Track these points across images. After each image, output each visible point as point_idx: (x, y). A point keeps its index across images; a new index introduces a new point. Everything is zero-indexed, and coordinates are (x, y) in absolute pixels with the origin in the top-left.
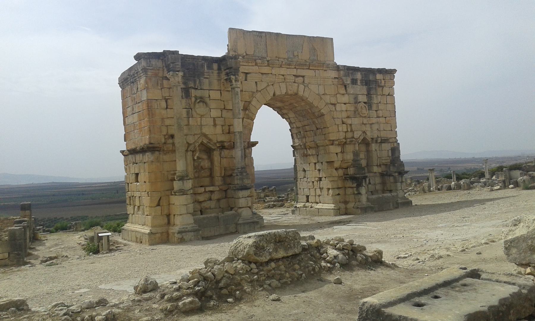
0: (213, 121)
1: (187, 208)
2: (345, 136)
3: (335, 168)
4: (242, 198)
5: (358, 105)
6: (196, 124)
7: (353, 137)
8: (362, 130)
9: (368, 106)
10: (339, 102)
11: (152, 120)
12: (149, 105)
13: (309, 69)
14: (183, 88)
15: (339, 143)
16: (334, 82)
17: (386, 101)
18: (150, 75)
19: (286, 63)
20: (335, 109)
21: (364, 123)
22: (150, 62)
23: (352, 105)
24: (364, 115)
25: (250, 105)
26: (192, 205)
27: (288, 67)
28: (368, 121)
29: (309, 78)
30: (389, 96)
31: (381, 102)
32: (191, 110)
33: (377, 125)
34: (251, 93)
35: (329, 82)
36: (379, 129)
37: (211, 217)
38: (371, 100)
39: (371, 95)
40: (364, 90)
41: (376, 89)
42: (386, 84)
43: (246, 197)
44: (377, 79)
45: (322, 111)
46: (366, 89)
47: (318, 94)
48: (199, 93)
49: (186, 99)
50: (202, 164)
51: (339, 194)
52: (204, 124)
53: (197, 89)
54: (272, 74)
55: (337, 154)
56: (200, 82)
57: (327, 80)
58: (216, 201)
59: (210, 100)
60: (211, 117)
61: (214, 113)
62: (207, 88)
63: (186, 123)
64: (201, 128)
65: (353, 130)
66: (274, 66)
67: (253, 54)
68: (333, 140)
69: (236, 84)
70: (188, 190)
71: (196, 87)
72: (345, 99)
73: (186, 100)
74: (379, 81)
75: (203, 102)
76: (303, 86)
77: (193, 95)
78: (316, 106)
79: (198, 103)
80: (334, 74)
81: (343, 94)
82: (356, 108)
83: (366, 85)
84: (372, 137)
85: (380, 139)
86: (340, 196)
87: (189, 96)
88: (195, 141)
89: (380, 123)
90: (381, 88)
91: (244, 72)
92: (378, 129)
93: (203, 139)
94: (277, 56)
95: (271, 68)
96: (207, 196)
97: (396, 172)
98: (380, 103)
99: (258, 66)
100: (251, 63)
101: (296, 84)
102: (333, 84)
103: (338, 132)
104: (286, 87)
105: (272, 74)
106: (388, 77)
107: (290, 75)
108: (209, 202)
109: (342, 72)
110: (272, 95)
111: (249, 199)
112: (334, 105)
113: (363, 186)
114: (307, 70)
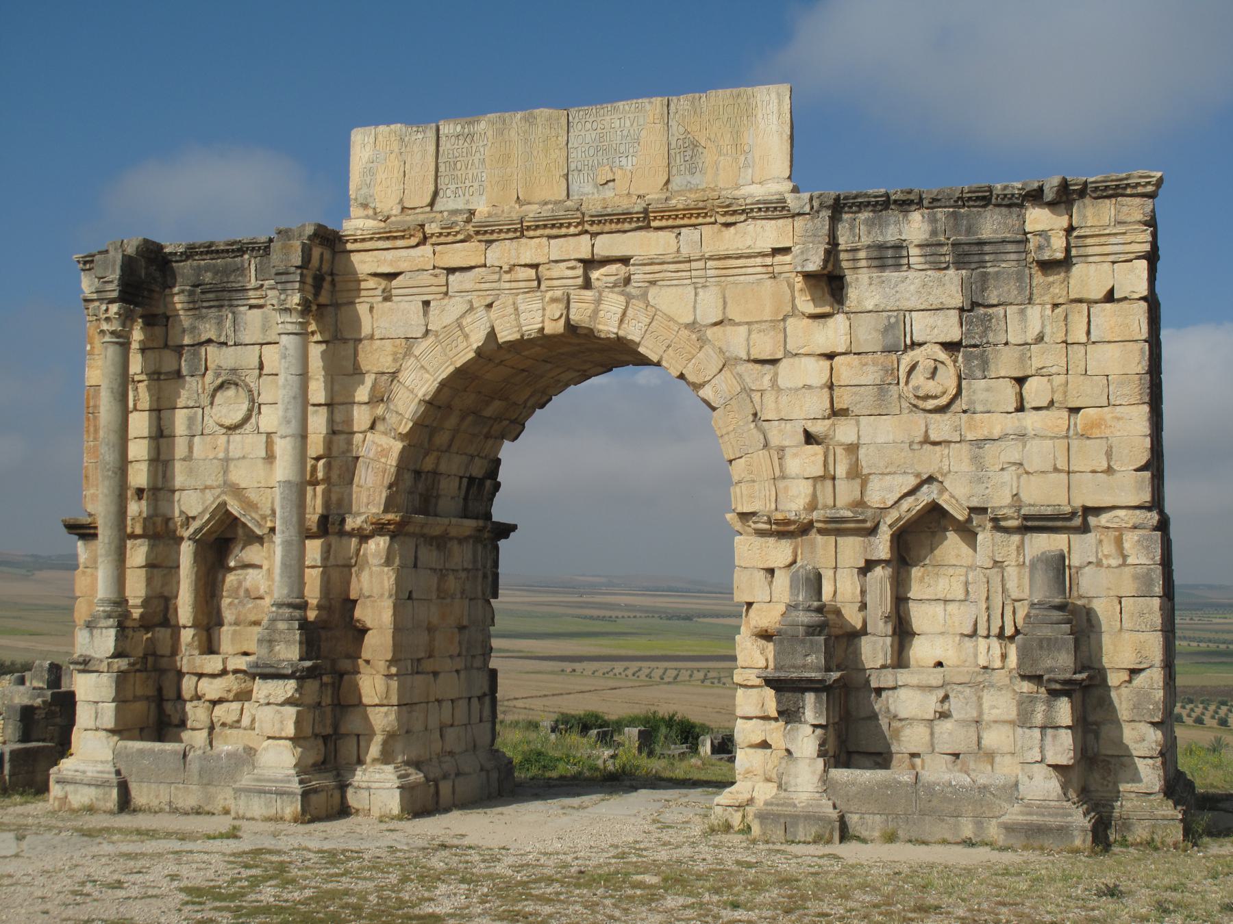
0: (263, 446)
1: (97, 713)
2: (814, 496)
4: (268, 704)
6: (211, 457)
7: (860, 504)
8: (920, 469)
9: (968, 359)
11: (94, 446)
12: (91, 404)
13: (648, 227)
16: (777, 269)
17: (1088, 333)
20: (774, 381)
21: (934, 437)
24: (931, 404)
26: (114, 704)
27: (555, 232)
28: (957, 428)
30: (1108, 305)
32: (200, 411)
35: (750, 270)
37: (163, 751)
38: (987, 329)
42: (1090, 251)
46: (957, 281)
47: (692, 326)
51: (765, 745)
53: (225, 344)
55: (771, 571)
59: (260, 375)
60: (261, 430)
65: (865, 471)
66: (495, 236)
70: (101, 661)
71: (222, 339)
72: (834, 334)
76: (622, 299)
82: (893, 371)
83: (959, 264)
84: (975, 503)
86: (769, 751)
91: (380, 270)
93: (224, 504)
98: (1040, 339)
101: (588, 294)
103: (784, 477)
108: (236, 706)
110: (477, 339)
112: (774, 362)
113: (806, 722)
114: (643, 233)
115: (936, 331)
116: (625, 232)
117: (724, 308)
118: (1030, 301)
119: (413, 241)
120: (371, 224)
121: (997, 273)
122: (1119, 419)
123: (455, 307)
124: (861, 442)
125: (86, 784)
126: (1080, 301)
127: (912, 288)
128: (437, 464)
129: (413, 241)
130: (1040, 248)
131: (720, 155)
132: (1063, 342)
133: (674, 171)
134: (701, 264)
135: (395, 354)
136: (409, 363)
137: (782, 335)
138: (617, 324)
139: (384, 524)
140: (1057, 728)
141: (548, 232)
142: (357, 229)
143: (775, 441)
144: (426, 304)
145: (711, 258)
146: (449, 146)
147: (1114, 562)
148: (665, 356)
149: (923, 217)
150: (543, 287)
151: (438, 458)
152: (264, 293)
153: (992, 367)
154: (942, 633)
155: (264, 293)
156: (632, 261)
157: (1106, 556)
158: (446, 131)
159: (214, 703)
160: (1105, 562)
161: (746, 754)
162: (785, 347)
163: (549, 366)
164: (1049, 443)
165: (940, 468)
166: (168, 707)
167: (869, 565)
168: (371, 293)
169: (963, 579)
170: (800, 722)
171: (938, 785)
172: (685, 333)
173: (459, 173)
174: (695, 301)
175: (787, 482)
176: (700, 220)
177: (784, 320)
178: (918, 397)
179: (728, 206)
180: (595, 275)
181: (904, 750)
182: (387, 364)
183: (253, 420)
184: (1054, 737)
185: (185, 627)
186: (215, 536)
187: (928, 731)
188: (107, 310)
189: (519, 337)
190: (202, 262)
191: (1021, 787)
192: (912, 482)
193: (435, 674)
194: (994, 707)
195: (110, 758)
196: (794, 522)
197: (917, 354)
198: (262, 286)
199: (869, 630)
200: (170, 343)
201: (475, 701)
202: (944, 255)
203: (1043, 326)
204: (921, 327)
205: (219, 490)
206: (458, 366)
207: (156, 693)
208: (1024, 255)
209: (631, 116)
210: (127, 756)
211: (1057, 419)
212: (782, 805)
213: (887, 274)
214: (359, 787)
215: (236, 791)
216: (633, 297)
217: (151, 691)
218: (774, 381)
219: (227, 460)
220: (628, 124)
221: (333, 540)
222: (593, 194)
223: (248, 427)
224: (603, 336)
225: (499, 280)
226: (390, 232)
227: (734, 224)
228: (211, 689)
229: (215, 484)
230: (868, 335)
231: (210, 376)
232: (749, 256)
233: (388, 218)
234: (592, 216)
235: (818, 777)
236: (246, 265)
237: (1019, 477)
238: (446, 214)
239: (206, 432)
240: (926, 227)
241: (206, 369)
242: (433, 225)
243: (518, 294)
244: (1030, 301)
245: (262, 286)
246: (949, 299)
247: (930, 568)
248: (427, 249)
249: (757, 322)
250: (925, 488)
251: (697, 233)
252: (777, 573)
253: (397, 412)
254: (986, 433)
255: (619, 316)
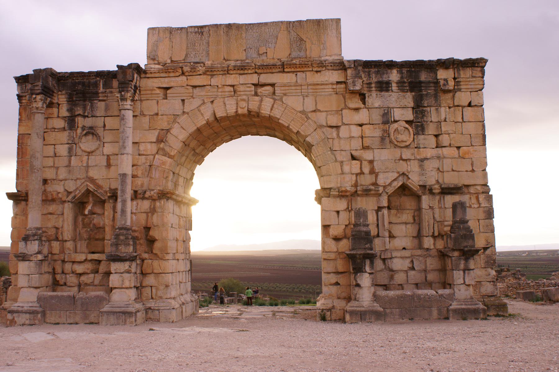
0: (105, 161)
2: (356, 181)
3: (331, 236)
4: (116, 273)
5: (392, 126)
7: (375, 184)
8: (399, 170)
9: (417, 127)
10: (345, 121)
11: (22, 161)
12: (20, 142)
13: (283, 72)
14: (68, 117)
15: (340, 193)
17: (463, 118)
18: (26, 104)
19: (235, 66)
20: (338, 135)
21: (404, 157)
22: (26, 87)
23: (377, 126)
24: (403, 144)
25: (169, 135)
26: (38, 275)
27: (242, 72)
28: (413, 154)
29: (283, 86)
30: (469, 108)
31: (447, 120)
32: (75, 146)
33: (438, 161)
34: (173, 116)
36: (441, 169)
37: (62, 296)
38: (423, 116)
39: (425, 107)
40: (409, 99)
41: (436, 96)
42: (462, 87)
43: (122, 273)
44: (438, 78)
45: (308, 139)
46: (411, 97)
47: (303, 112)
48: (89, 122)
49: (69, 131)
50: (95, 221)
51: (337, 284)
52: (93, 165)
53: (87, 116)
54: (210, 85)
56: (92, 107)
57: (322, 87)
58: (102, 275)
59: (104, 130)
60: (105, 154)
61: (108, 149)
62: (102, 113)
63: (66, 162)
64: (88, 169)
65: (377, 171)
66: (215, 73)
67: (184, 60)
68: (330, 189)
69: (122, 105)
70: (31, 255)
71: (86, 114)
72: (363, 116)
73: (69, 133)
74: (442, 82)
75: (93, 134)
76: (271, 100)
77: (80, 125)
78: (296, 131)
79: (86, 135)
80: (335, 76)
81: (357, 109)
83: (411, 91)
84: (421, 183)
85: (437, 186)
86: (339, 286)
87: (74, 126)
88: (77, 189)
89: (444, 157)
90: (451, 94)
92: (438, 169)
93: (87, 185)
94: (226, 58)
95: (210, 77)
96: (88, 267)
97: (453, 250)
98: (445, 121)
99: (186, 76)
100: (173, 72)
101: (257, 98)
102: (337, 93)
103: (343, 173)
104: (237, 104)
105: (210, 85)
106: (465, 74)
107: (246, 84)
108: (92, 276)
109: (349, 72)
110: (208, 115)
111: (126, 275)
112: (337, 127)
113: (366, 272)
114: (281, 74)
115: (403, 116)
116: (273, 73)
117: (316, 105)
118: (440, 106)
119: (177, 74)
120: (157, 66)
121: (427, 94)
122: (475, 151)
123: (196, 102)
124: (375, 159)
125: (24, 313)
126: (458, 106)
127: (393, 99)
128: (180, 171)
129: (177, 74)
130: (444, 85)
131: (312, 44)
132: (453, 121)
133: (293, 50)
134: (306, 87)
135: (168, 121)
136: (175, 125)
137: (340, 117)
138: (269, 110)
139: (165, 194)
140: (469, 270)
141: (239, 72)
142: (152, 68)
143: (339, 158)
144: (183, 101)
145: (310, 85)
146: (192, 36)
147: (476, 206)
148: (291, 124)
149: (398, 72)
150: (236, 95)
151: (180, 168)
152: (106, 95)
153: (426, 131)
154: (405, 236)
155: (106, 95)
156: (276, 85)
157: (473, 204)
158: (190, 30)
159: (81, 274)
160: (472, 206)
161: (329, 288)
162: (342, 121)
163: (225, 132)
164: (450, 160)
165: (407, 170)
166: (58, 277)
167: (380, 209)
168: (157, 96)
169: (413, 214)
170: (363, 272)
171: (422, 295)
172: (299, 114)
173: (197, 48)
174: (303, 102)
175: (344, 175)
176: (306, 69)
177: (341, 110)
178: (397, 141)
179: (318, 64)
180: (260, 90)
181: (396, 283)
182: (165, 126)
183: (101, 149)
184: (468, 274)
185: (66, 241)
186: (79, 201)
187: (406, 275)
188: (35, 98)
189: (226, 115)
190: (77, 81)
191: (456, 294)
192: (396, 175)
193: (178, 260)
194: (431, 264)
195: (36, 300)
196: (349, 191)
197: (395, 125)
198: (106, 91)
199: (380, 235)
200: (60, 115)
201: (187, 272)
202: (406, 87)
203: (446, 115)
204: (397, 114)
205: (84, 180)
206: (199, 126)
207: (52, 271)
208: (436, 89)
209: (274, 27)
210: (44, 299)
211: (453, 152)
212: (358, 307)
213: (383, 93)
214: (154, 310)
215: (102, 312)
216: (276, 100)
217: (51, 270)
218: (338, 135)
219: (88, 166)
220: (272, 30)
221: (140, 201)
222: (257, 58)
223: (98, 152)
224: (263, 115)
225: (217, 91)
226: (168, 70)
227: (320, 71)
228: (79, 269)
229: (82, 177)
230: (377, 117)
231: (79, 131)
232: (327, 84)
233: (166, 64)
234: (259, 66)
235: (372, 294)
236: (98, 82)
237: (438, 173)
238: (192, 64)
239: (78, 154)
240: (399, 75)
241: (78, 127)
242: (187, 68)
243: (225, 98)
244: (440, 106)
245: (106, 91)
246: (408, 104)
247: (399, 211)
248: (184, 78)
249: (330, 111)
250: (401, 178)
251: (304, 74)
252: (341, 213)
253: (170, 146)
254: (424, 156)
255: (269, 108)
